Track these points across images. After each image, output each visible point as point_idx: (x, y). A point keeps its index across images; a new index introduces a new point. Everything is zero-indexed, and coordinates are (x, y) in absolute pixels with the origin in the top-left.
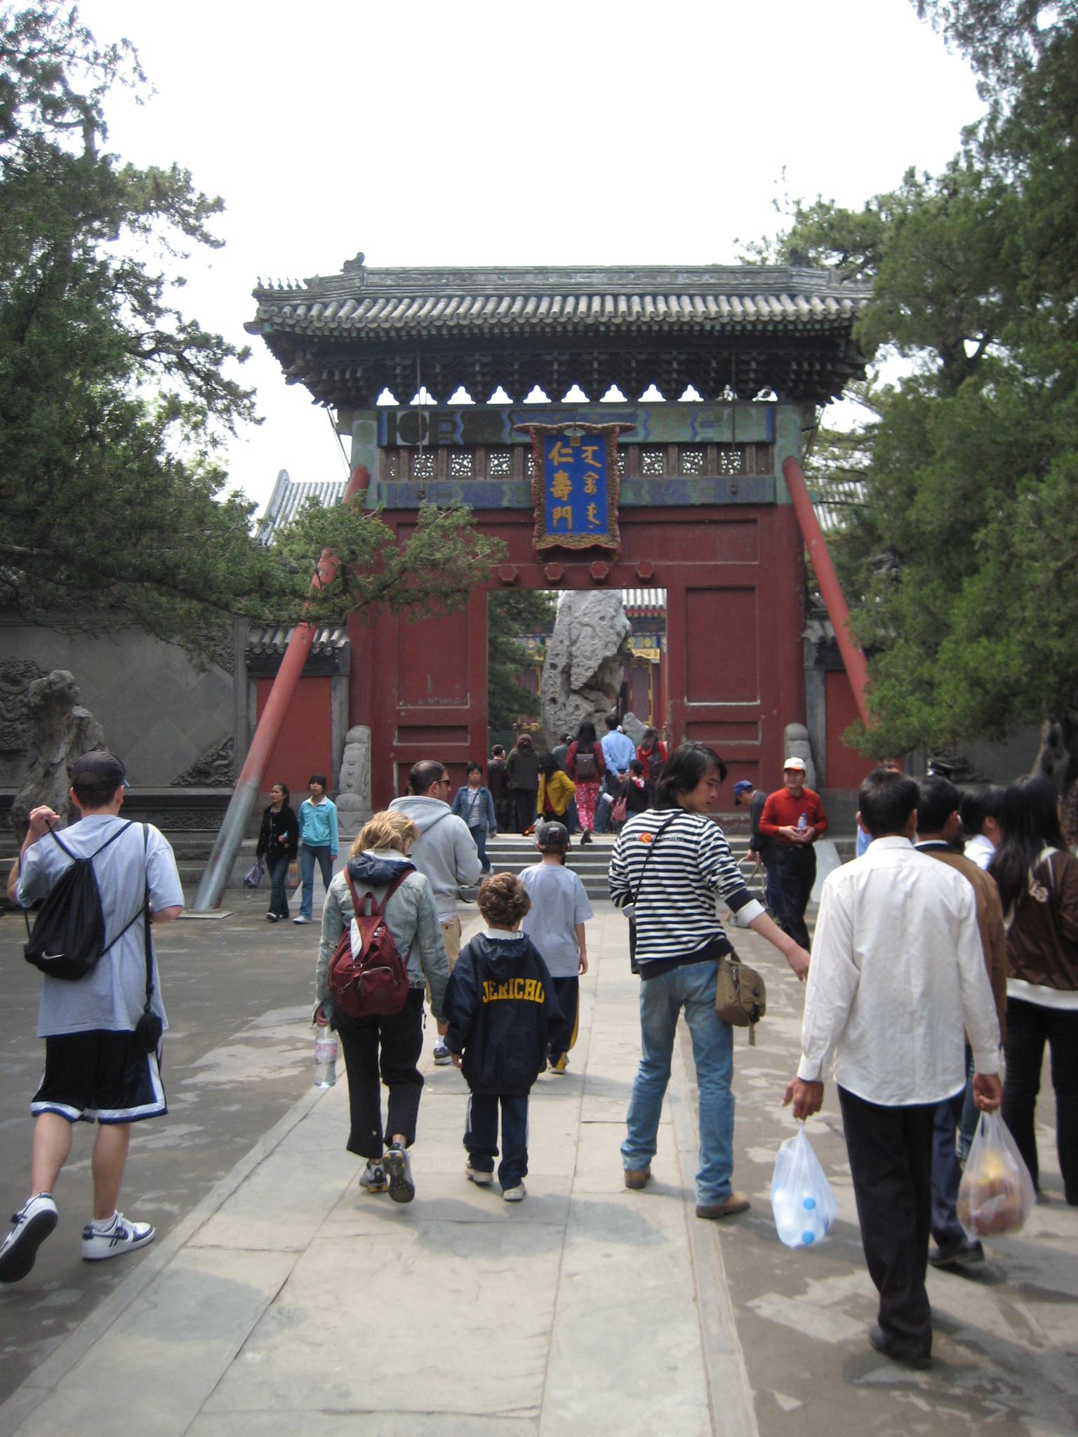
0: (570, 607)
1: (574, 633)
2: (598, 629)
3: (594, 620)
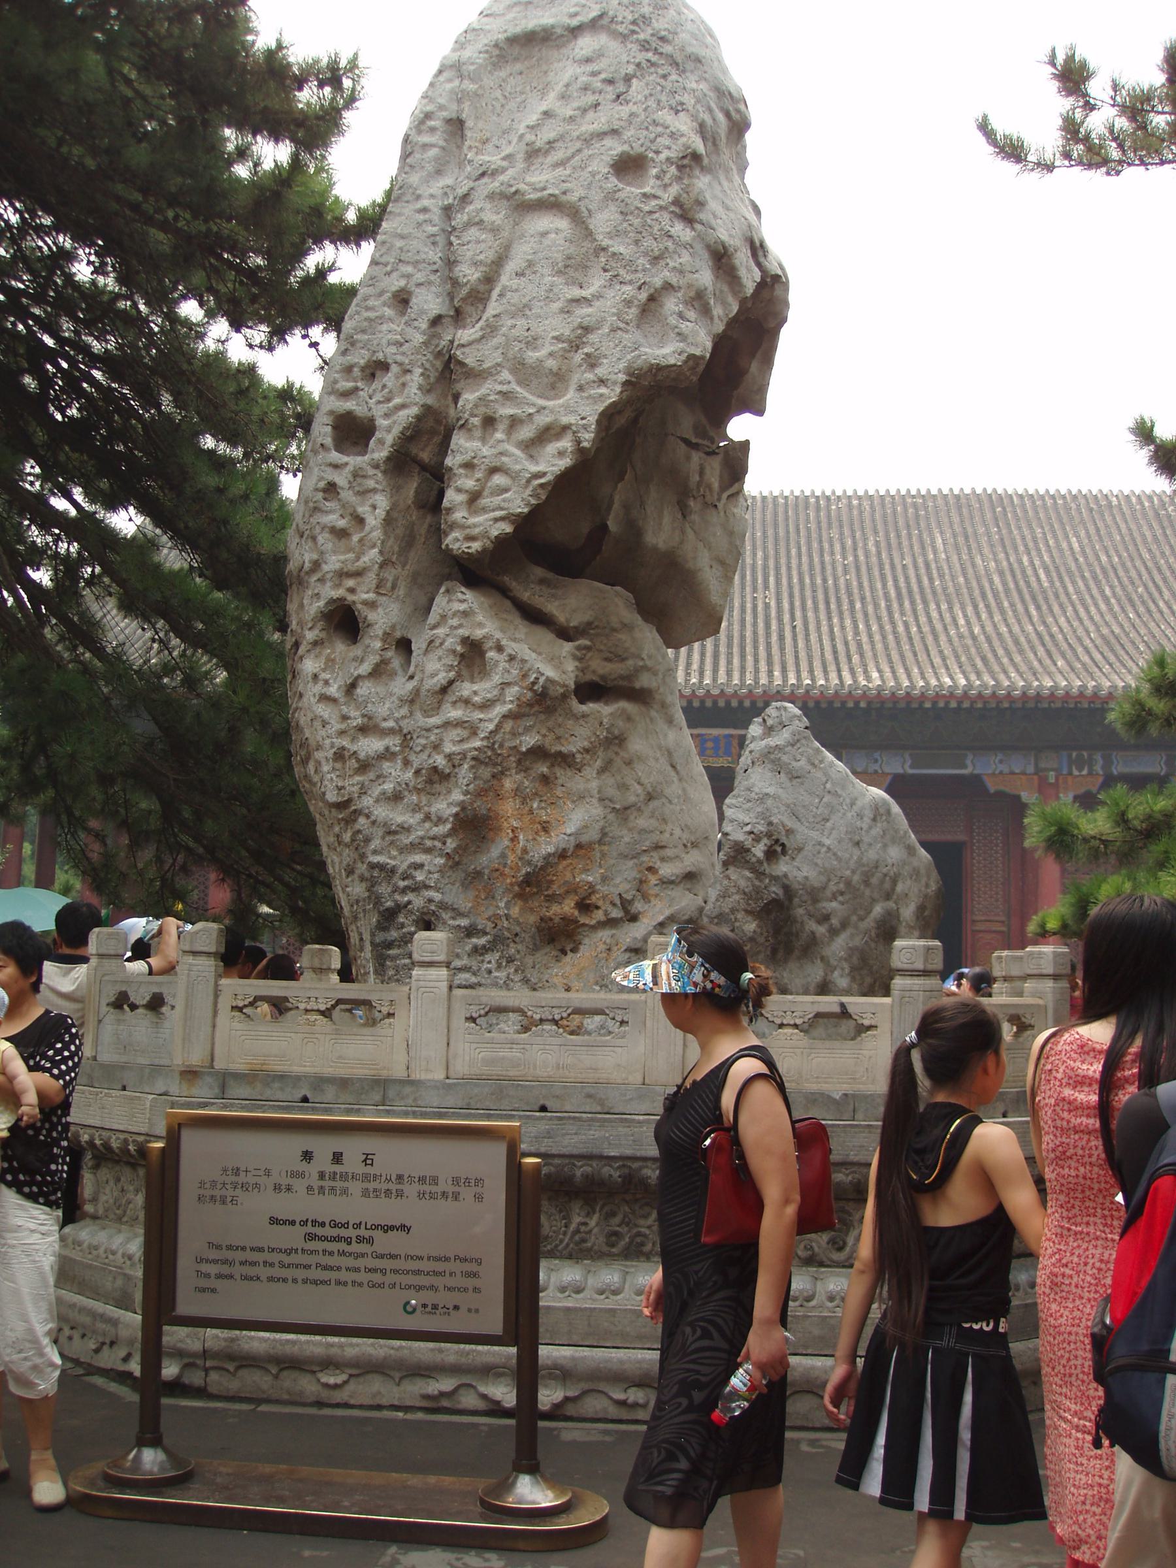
0: (457, 126)
1: (474, 252)
2: (603, 221)
3: (587, 177)
